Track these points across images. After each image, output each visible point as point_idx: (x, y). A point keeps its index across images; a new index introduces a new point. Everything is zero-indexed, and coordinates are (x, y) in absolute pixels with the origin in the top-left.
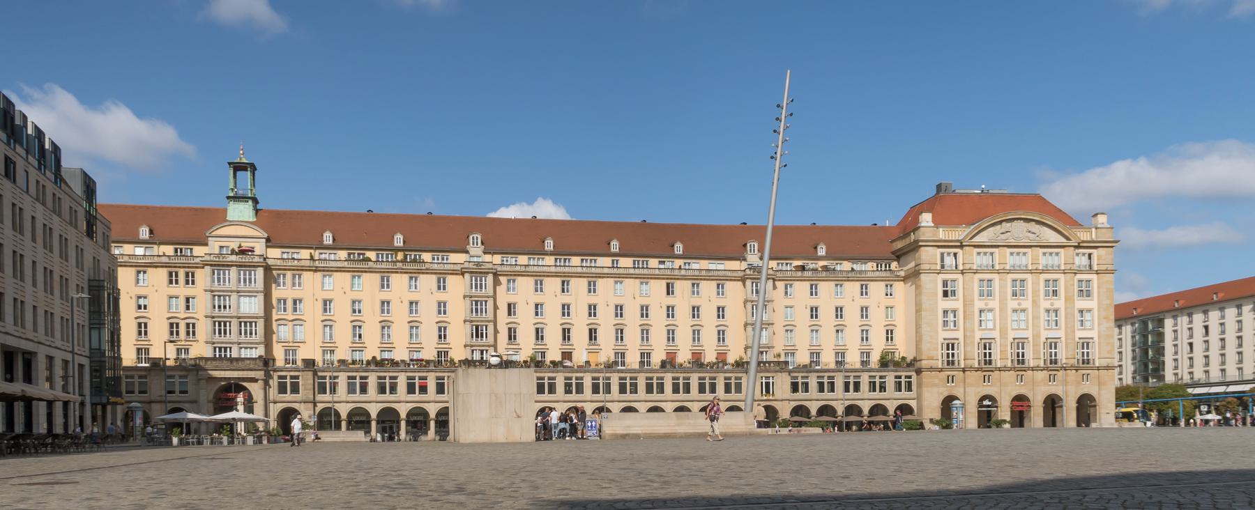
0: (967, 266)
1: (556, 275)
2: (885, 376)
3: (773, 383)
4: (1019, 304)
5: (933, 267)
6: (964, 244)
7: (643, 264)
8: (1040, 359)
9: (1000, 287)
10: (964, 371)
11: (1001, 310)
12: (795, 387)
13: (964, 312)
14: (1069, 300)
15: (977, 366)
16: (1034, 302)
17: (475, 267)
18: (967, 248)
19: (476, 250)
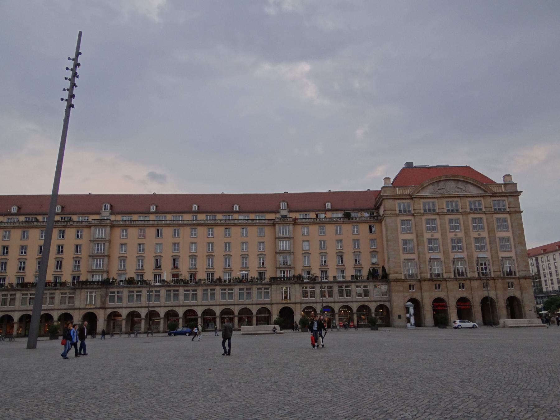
0: (417, 211)
1: (153, 226)
2: (367, 285)
3: (290, 291)
4: (456, 235)
5: (393, 212)
6: (413, 197)
7: (213, 218)
8: (475, 272)
9: (441, 224)
10: (420, 281)
11: (443, 239)
12: (305, 295)
13: (417, 241)
14: (491, 231)
15: (429, 277)
16: (466, 233)
17: (98, 222)
18: (415, 199)
19: (106, 214)
